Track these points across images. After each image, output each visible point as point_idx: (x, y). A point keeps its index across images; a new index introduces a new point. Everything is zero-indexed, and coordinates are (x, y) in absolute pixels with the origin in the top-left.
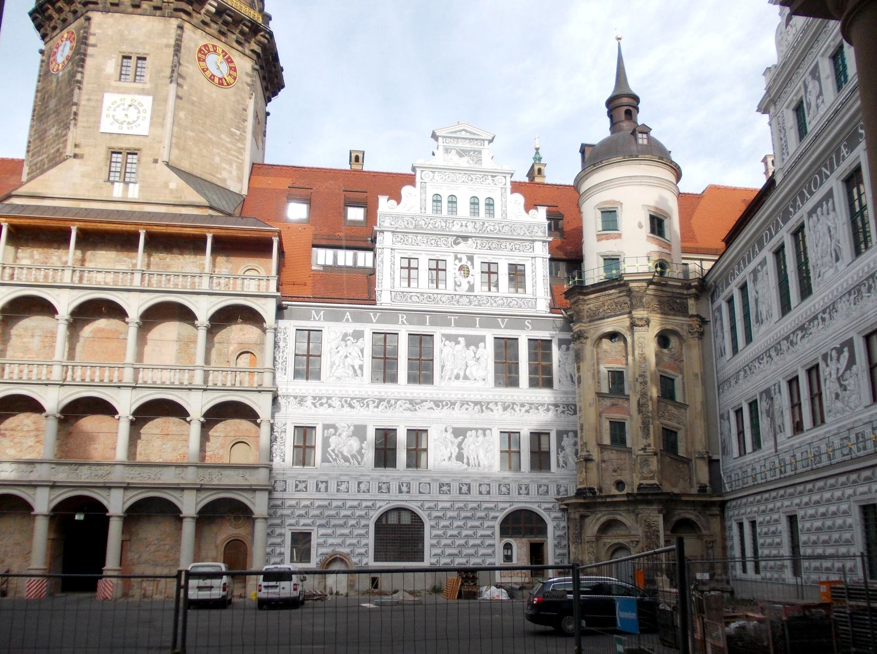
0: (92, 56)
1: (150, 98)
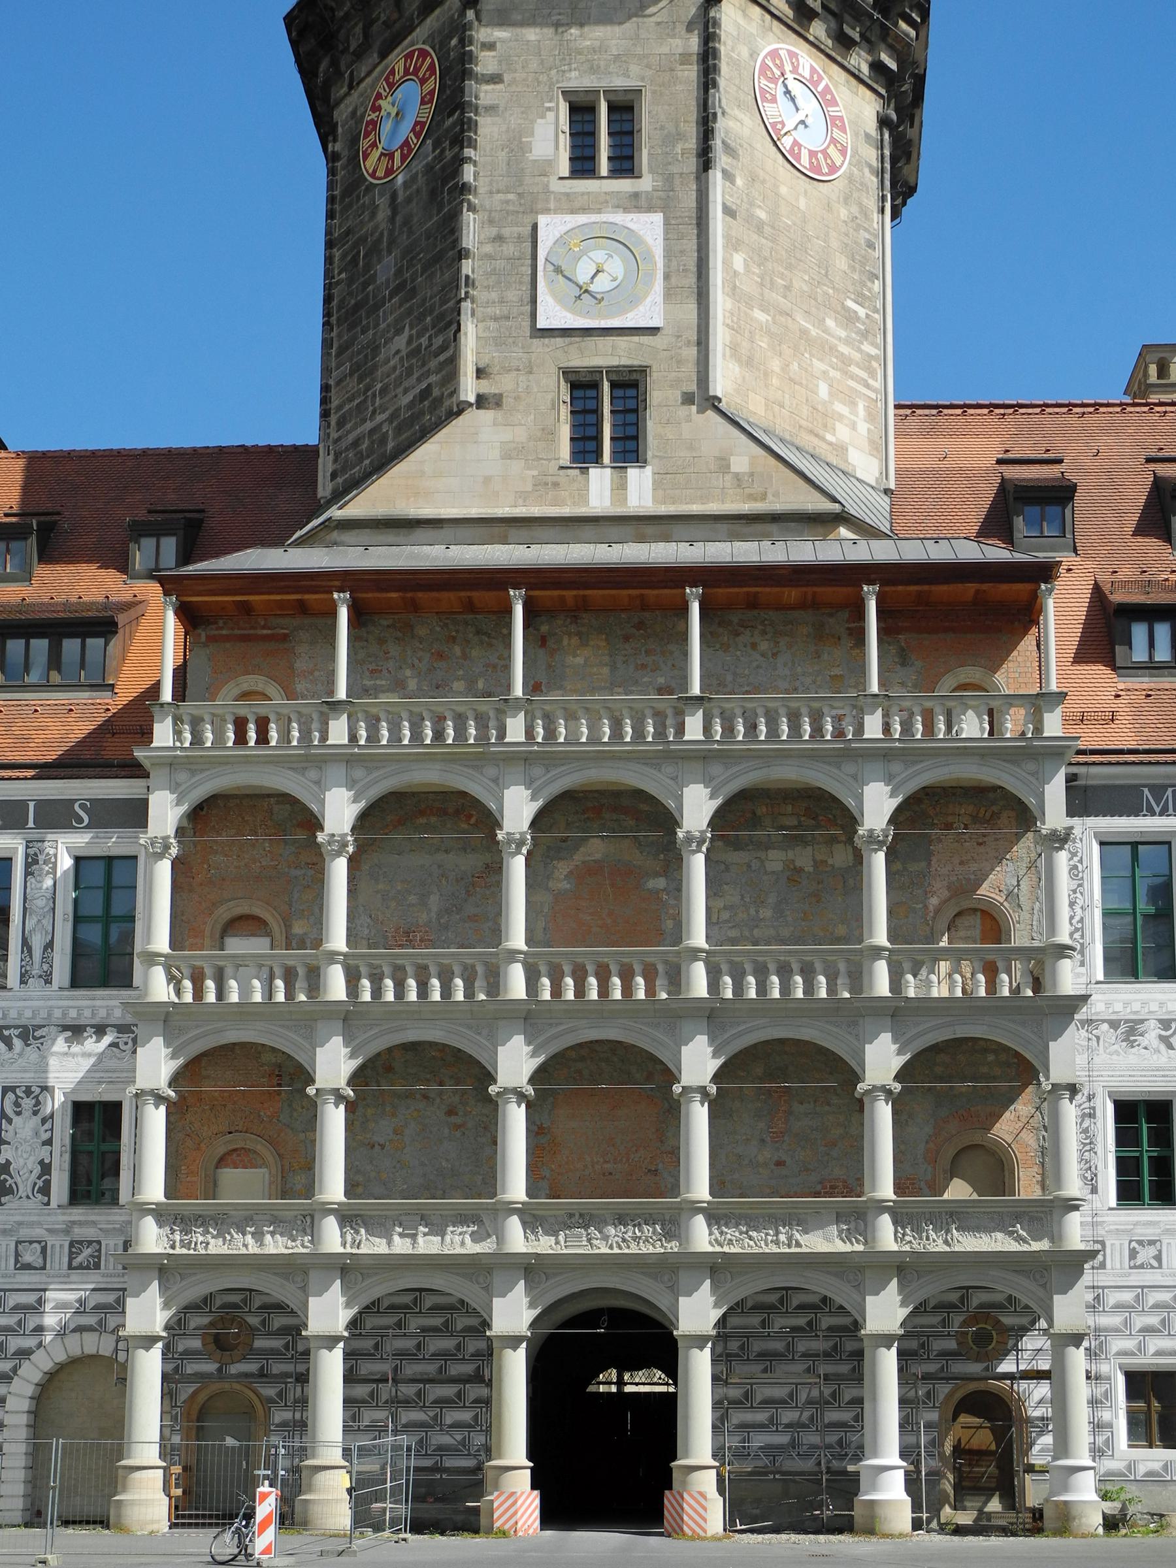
0: (492, 109)
1: (657, 219)
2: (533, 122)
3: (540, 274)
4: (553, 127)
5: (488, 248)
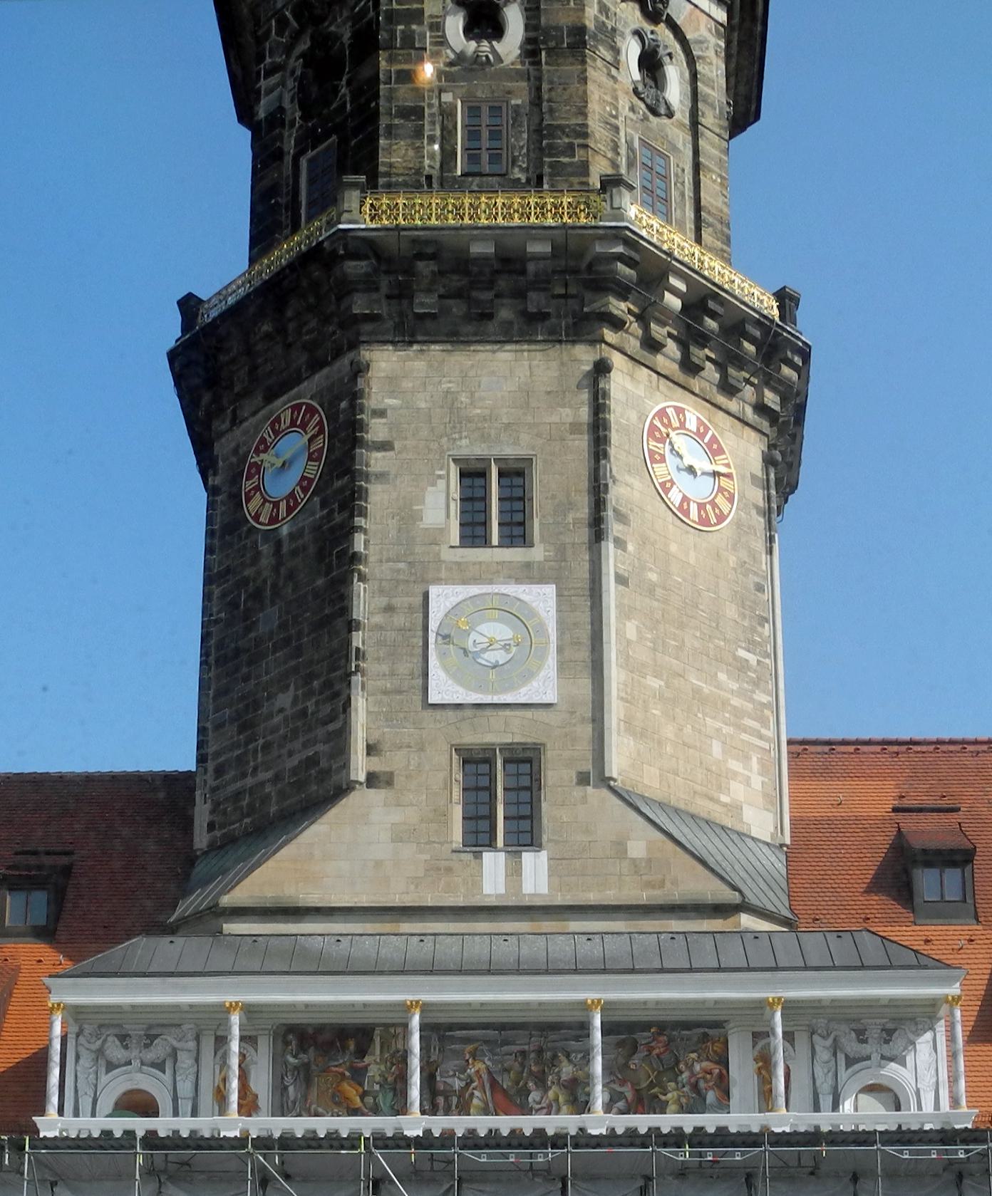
0: (382, 476)
1: (550, 590)
2: (424, 490)
3: (431, 646)
4: (444, 495)
5: (378, 619)
